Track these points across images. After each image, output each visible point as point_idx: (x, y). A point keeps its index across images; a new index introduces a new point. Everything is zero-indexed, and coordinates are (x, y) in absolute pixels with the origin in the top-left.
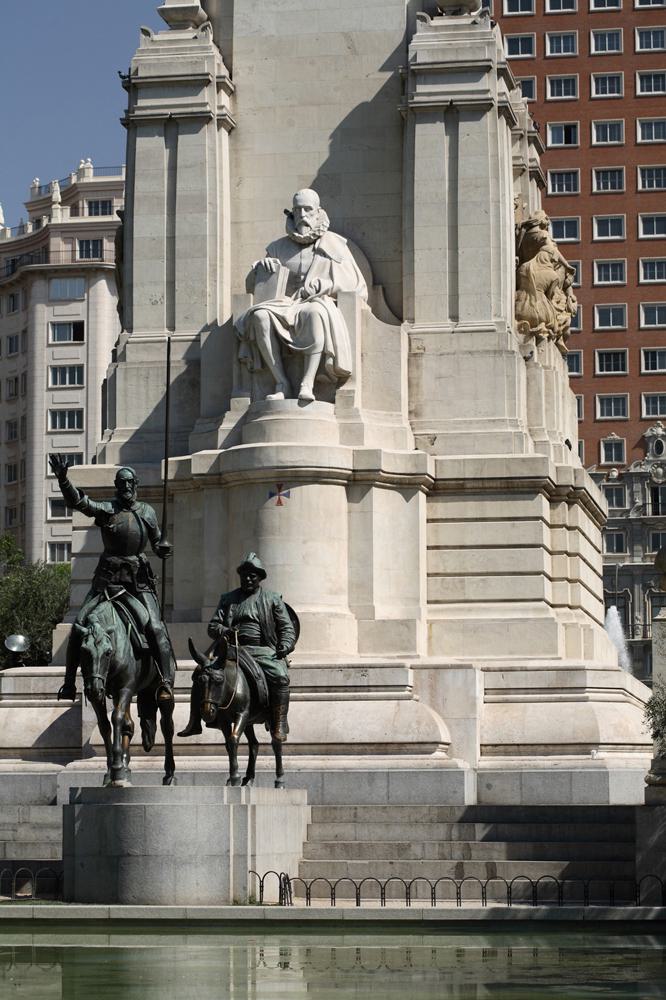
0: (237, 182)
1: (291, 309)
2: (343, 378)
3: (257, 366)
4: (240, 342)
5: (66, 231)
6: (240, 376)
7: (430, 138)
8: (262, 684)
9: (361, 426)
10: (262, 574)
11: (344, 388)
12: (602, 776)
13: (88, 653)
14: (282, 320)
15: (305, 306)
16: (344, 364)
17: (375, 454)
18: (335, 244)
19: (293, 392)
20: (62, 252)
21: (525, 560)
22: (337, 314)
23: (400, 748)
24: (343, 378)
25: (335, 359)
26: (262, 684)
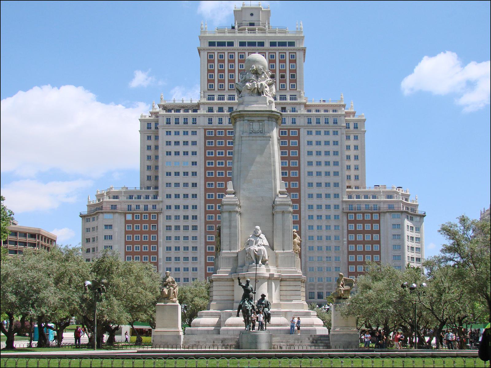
0: (241, 224)
1: (257, 248)
2: (266, 261)
3: (250, 258)
4: (247, 254)
5: (107, 202)
6: (247, 260)
7: (278, 217)
8: (267, 314)
9: (270, 269)
10: (265, 296)
11: (267, 262)
12: (315, 331)
13: (248, 309)
14: (255, 250)
15: (259, 248)
16: (267, 258)
17: (273, 274)
18: (262, 236)
19: (257, 263)
20: (106, 207)
21: (298, 293)
22: (265, 248)
23: (281, 325)
24: (266, 261)
25: (265, 257)
26: (267, 314)
